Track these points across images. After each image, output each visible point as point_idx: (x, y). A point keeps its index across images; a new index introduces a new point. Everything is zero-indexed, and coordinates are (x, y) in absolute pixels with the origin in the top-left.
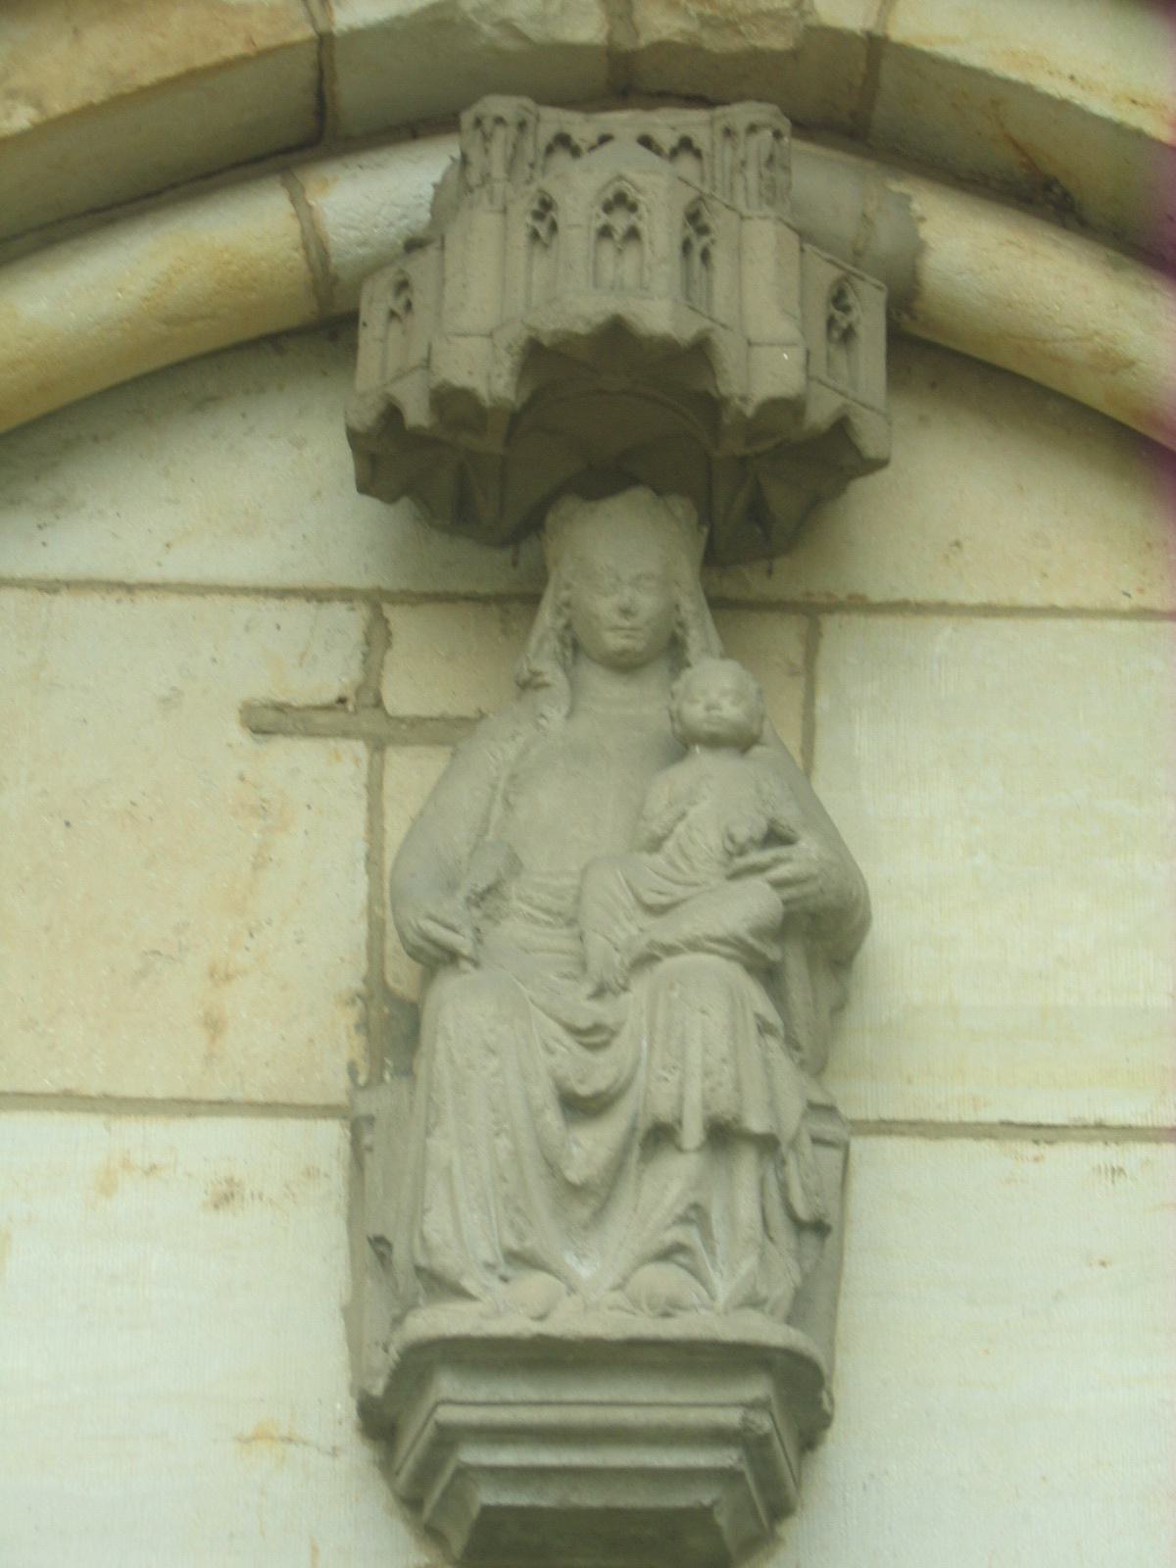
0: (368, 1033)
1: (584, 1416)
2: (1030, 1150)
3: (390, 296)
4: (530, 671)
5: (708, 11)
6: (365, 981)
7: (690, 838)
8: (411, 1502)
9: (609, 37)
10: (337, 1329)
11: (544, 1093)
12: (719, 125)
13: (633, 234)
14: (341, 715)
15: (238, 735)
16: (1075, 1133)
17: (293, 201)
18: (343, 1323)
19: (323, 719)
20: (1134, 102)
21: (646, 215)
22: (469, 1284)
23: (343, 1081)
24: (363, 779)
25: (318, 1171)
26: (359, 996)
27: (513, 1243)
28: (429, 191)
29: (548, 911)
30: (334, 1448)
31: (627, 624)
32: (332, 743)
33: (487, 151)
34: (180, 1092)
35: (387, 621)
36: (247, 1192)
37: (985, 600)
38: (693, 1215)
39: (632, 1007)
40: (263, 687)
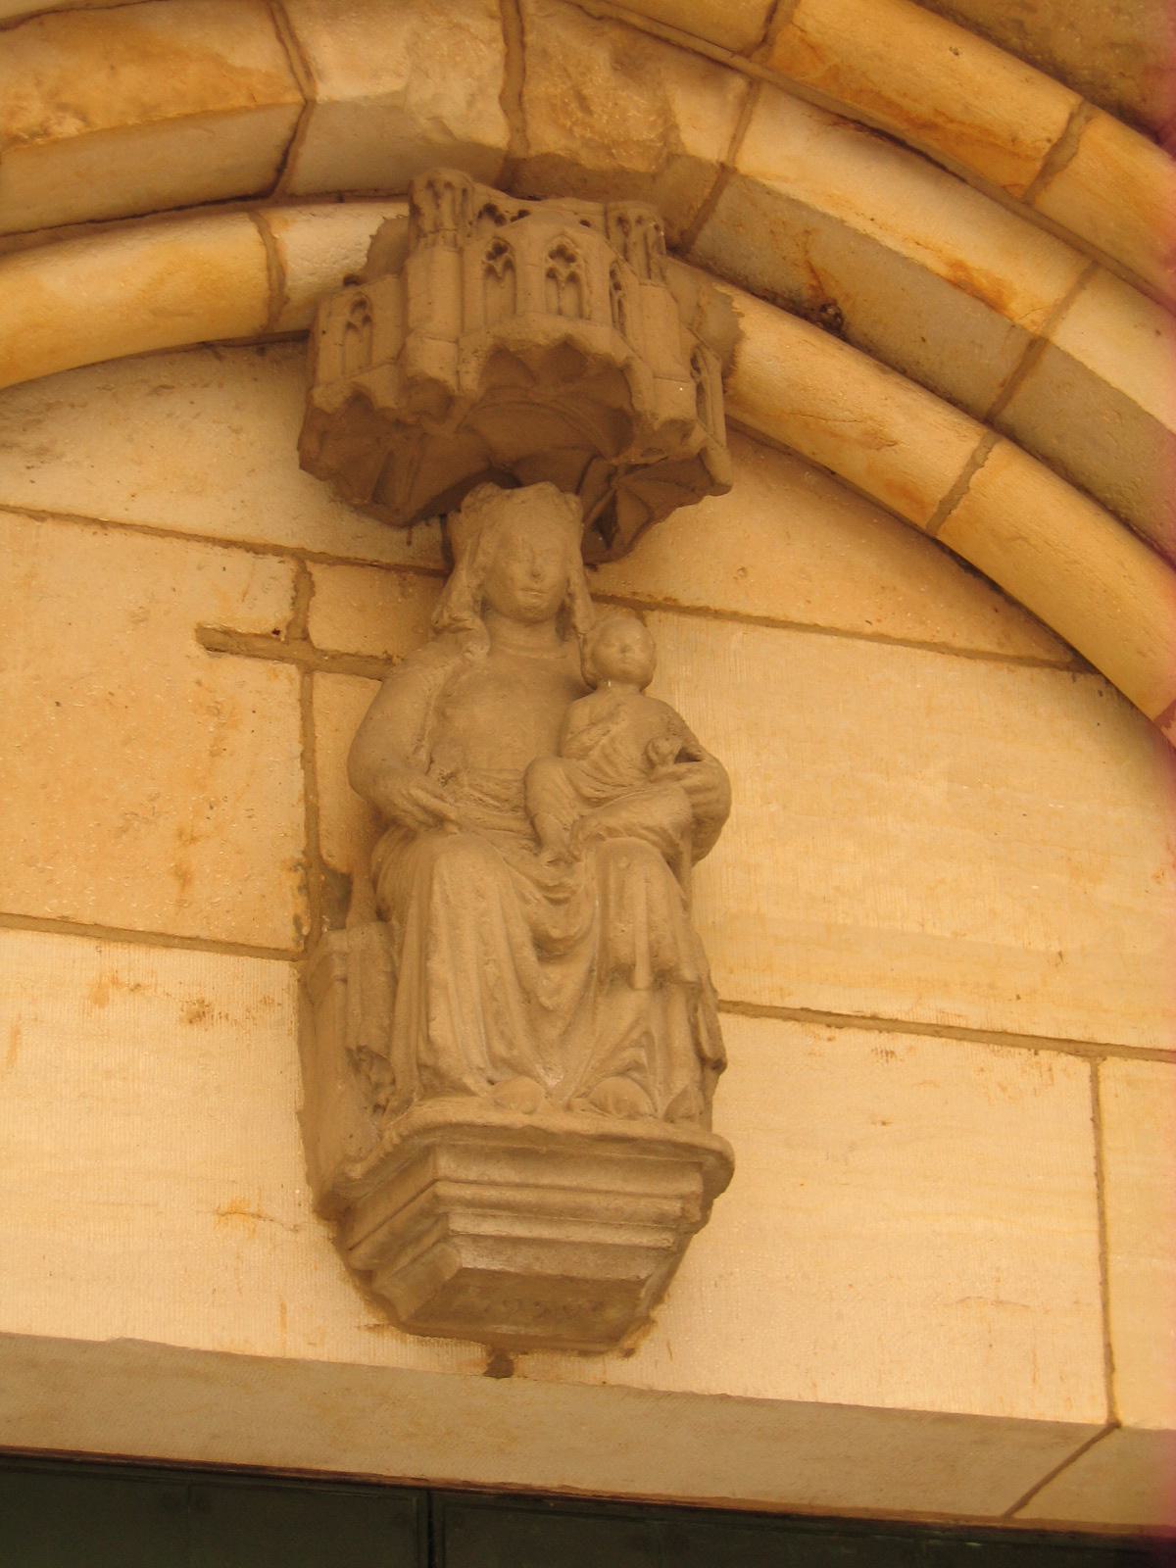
0: (309, 894)
1: (557, 1199)
2: (826, 1032)
3: (347, 311)
4: (450, 617)
5: (588, 135)
6: (304, 853)
7: (615, 750)
8: (365, 1278)
9: (509, 144)
10: (295, 1128)
11: (522, 935)
12: (614, 214)
13: (573, 279)
14: (276, 644)
15: (195, 649)
16: (856, 1022)
17: (261, 232)
18: (298, 1125)
19: (261, 644)
20: (918, 244)
21: (582, 263)
22: (469, 1081)
23: (290, 931)
24: (296, 695)
25: (273, 1000)
26: (300, 864)
27: (500, 1048)
28: (368, 241)
29: (495, 798)
30: (295, 1226)
31: (536, 586)
32: (270, 663)
33: (438, 206)
34: (157, 927)
35: (310, 574)
36: (216, 1013)
37: (765, 614)
38: (644, 1040)
39: (584, 876)
40: (213, 616)
